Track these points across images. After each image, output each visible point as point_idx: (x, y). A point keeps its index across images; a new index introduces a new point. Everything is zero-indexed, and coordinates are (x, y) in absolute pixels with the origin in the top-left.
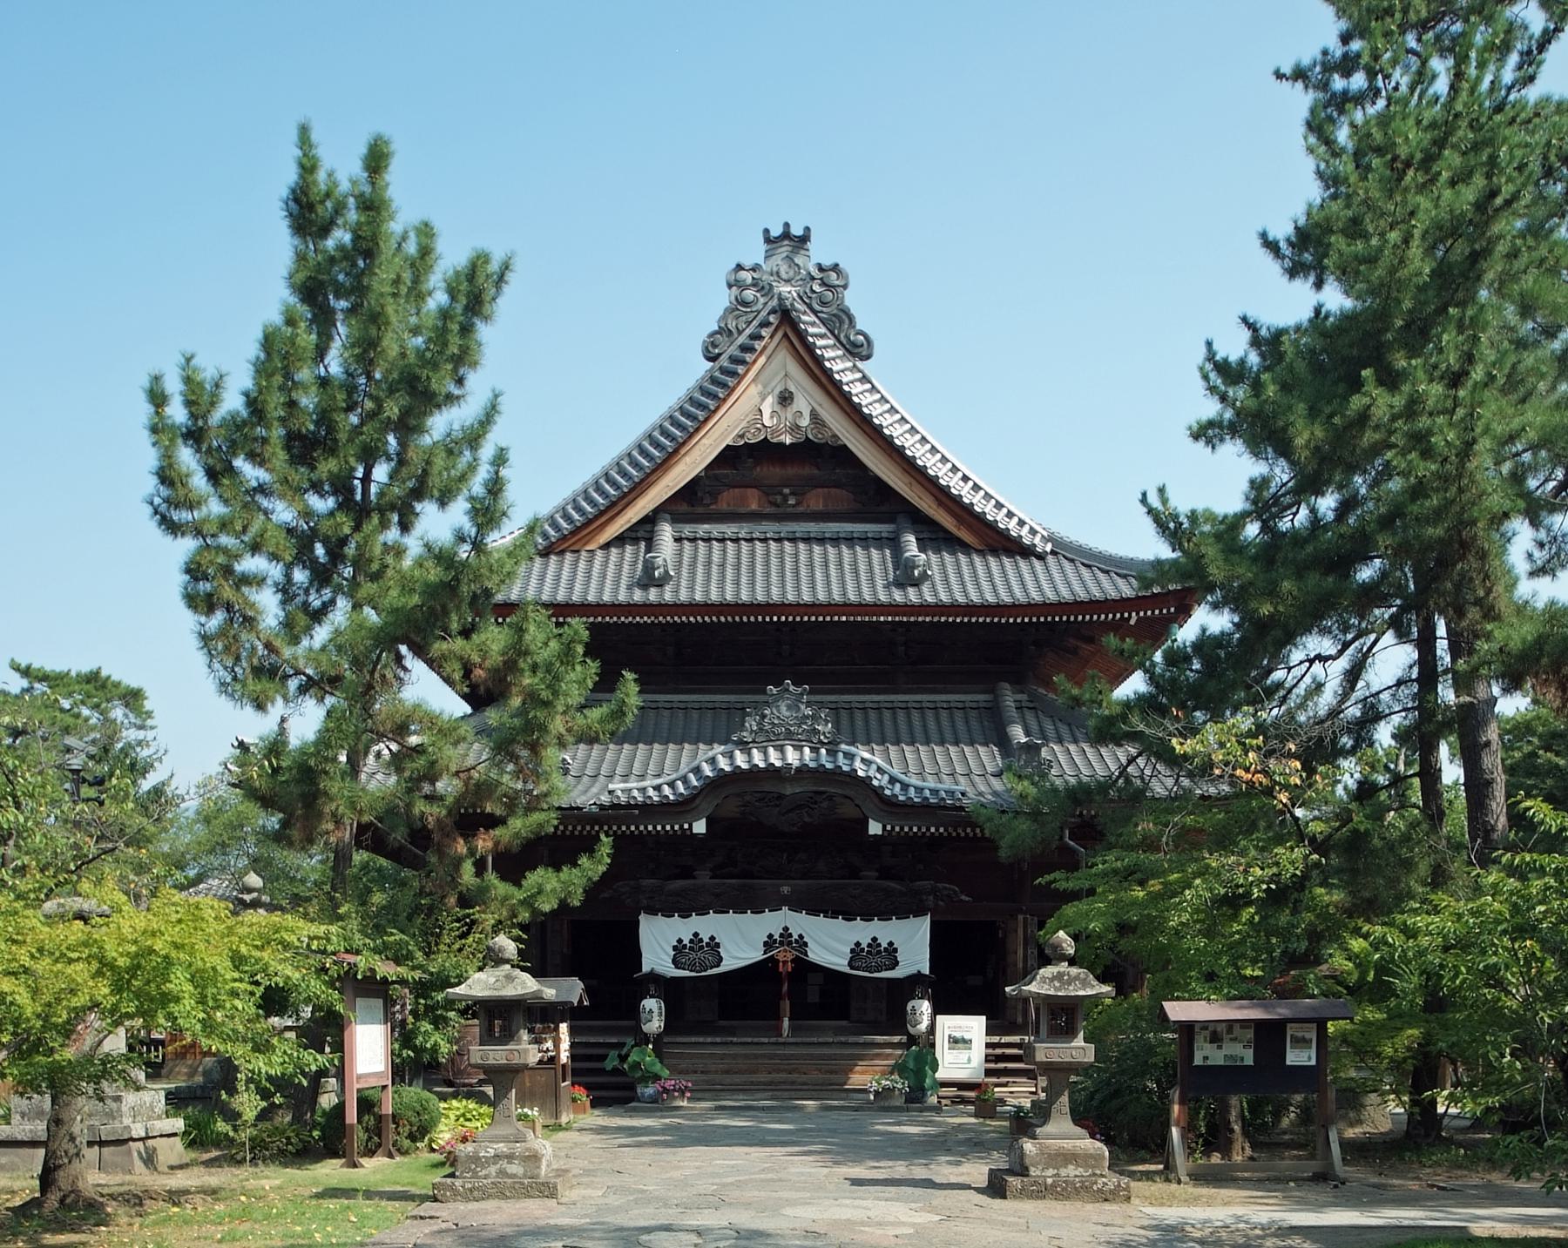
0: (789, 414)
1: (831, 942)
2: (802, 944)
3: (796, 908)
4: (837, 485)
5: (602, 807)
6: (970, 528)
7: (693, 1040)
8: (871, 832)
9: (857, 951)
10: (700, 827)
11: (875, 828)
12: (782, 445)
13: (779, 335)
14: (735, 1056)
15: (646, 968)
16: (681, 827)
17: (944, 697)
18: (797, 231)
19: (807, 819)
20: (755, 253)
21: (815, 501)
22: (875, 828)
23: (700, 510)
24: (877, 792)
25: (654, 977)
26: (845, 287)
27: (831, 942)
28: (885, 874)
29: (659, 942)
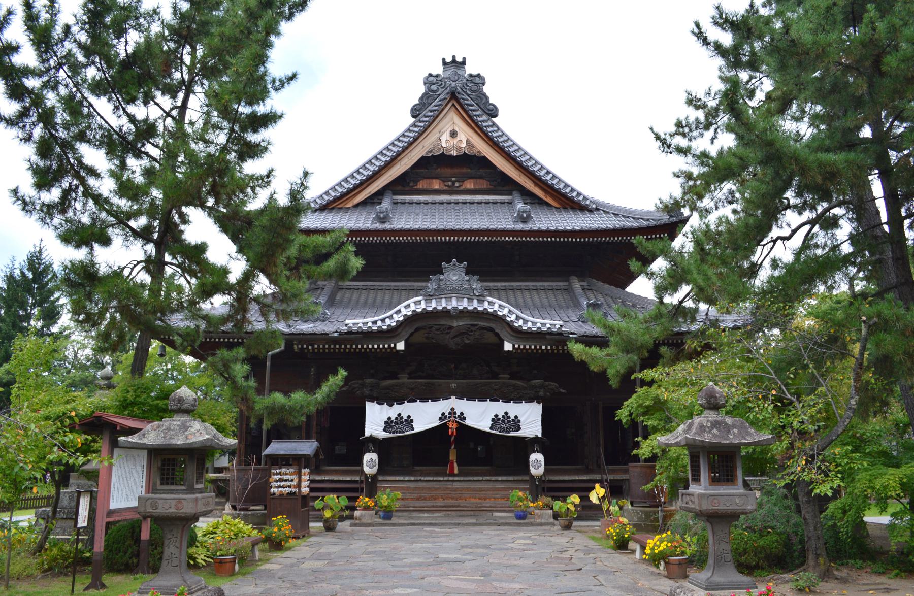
0: (455, 141)
1: (480, 415)
2: (462, 417)
3: (460, 396)
4: (481, 177)
5: (341, 333)
6: (552, 196)
7: (397, 478)
8: (851, 250)
9: (495, 420)
10: (401, 346)
11: (508, 347)
12: (451, 156)
13: (450, 104)
14: (423, 489)
15: (367, 434)
16: (389, 346)
17: (541, 284)
18: (459, 59)
19: (467, 342)
20: (438, 69)
21: (469, 185)
22: (508, 347)
23: (407, 189)
24: (510, 325)
25: (372, 439)
26: (484, 84)
27: (480, 415)
28: (513, 376)
29: (376, 419)
